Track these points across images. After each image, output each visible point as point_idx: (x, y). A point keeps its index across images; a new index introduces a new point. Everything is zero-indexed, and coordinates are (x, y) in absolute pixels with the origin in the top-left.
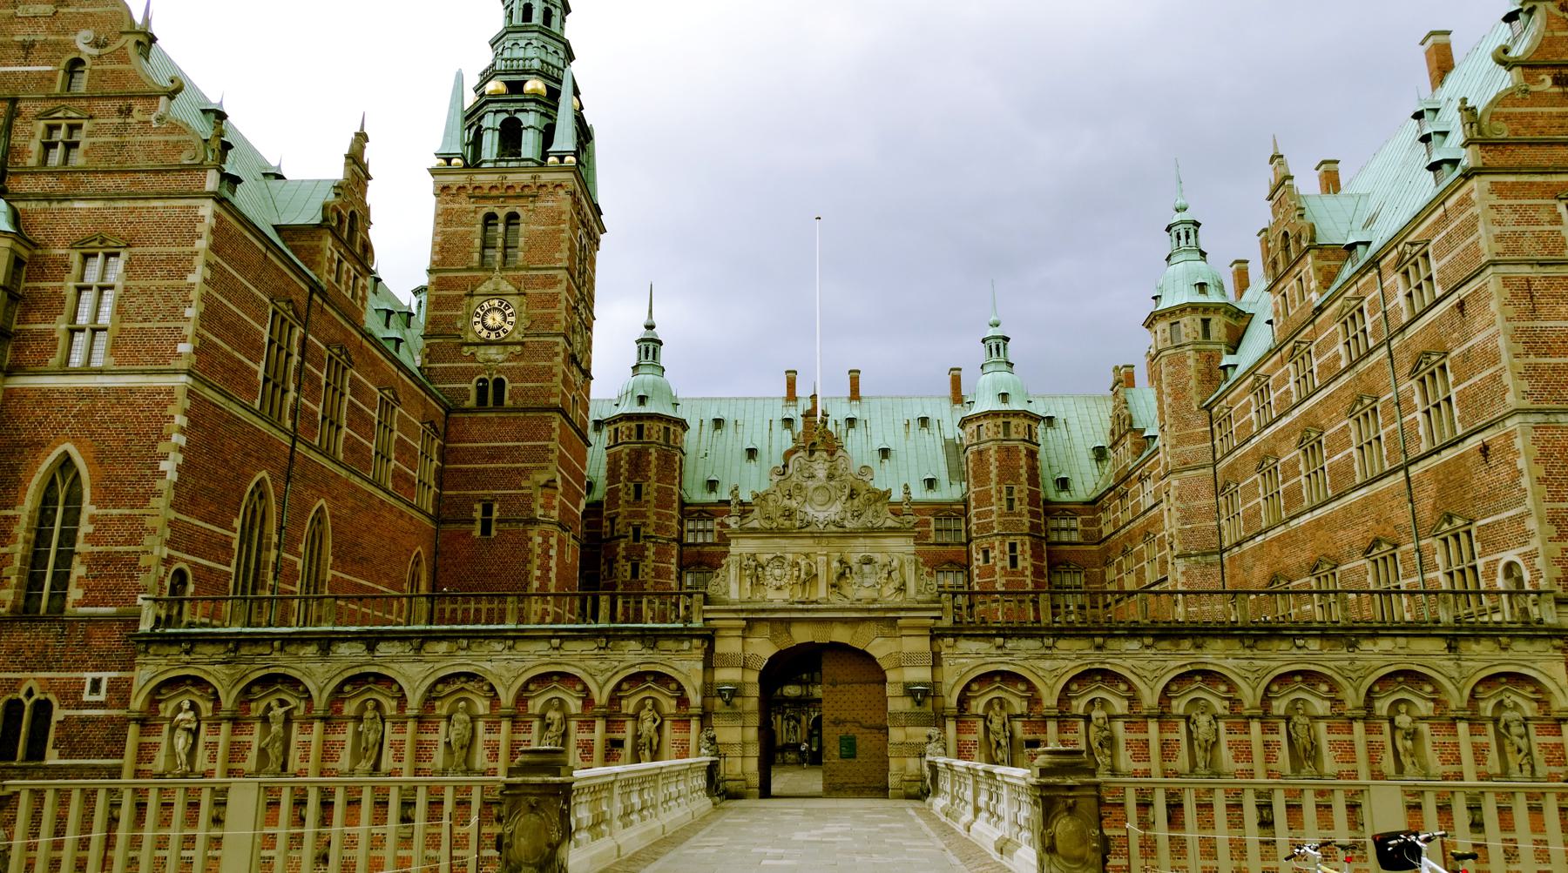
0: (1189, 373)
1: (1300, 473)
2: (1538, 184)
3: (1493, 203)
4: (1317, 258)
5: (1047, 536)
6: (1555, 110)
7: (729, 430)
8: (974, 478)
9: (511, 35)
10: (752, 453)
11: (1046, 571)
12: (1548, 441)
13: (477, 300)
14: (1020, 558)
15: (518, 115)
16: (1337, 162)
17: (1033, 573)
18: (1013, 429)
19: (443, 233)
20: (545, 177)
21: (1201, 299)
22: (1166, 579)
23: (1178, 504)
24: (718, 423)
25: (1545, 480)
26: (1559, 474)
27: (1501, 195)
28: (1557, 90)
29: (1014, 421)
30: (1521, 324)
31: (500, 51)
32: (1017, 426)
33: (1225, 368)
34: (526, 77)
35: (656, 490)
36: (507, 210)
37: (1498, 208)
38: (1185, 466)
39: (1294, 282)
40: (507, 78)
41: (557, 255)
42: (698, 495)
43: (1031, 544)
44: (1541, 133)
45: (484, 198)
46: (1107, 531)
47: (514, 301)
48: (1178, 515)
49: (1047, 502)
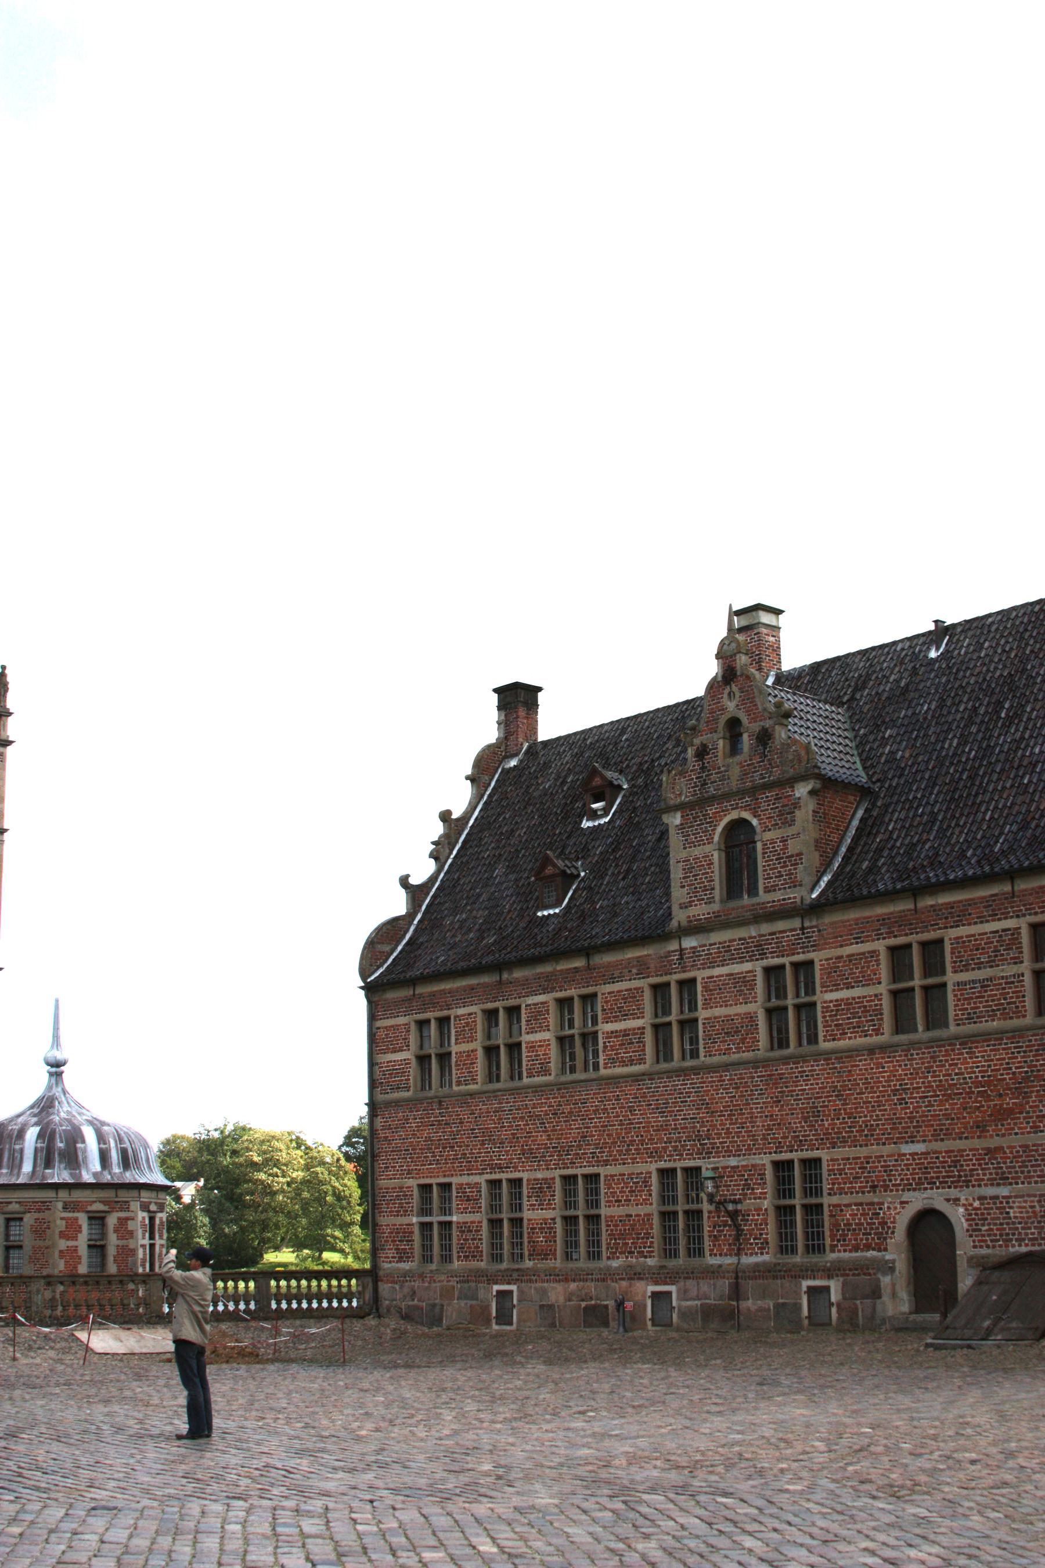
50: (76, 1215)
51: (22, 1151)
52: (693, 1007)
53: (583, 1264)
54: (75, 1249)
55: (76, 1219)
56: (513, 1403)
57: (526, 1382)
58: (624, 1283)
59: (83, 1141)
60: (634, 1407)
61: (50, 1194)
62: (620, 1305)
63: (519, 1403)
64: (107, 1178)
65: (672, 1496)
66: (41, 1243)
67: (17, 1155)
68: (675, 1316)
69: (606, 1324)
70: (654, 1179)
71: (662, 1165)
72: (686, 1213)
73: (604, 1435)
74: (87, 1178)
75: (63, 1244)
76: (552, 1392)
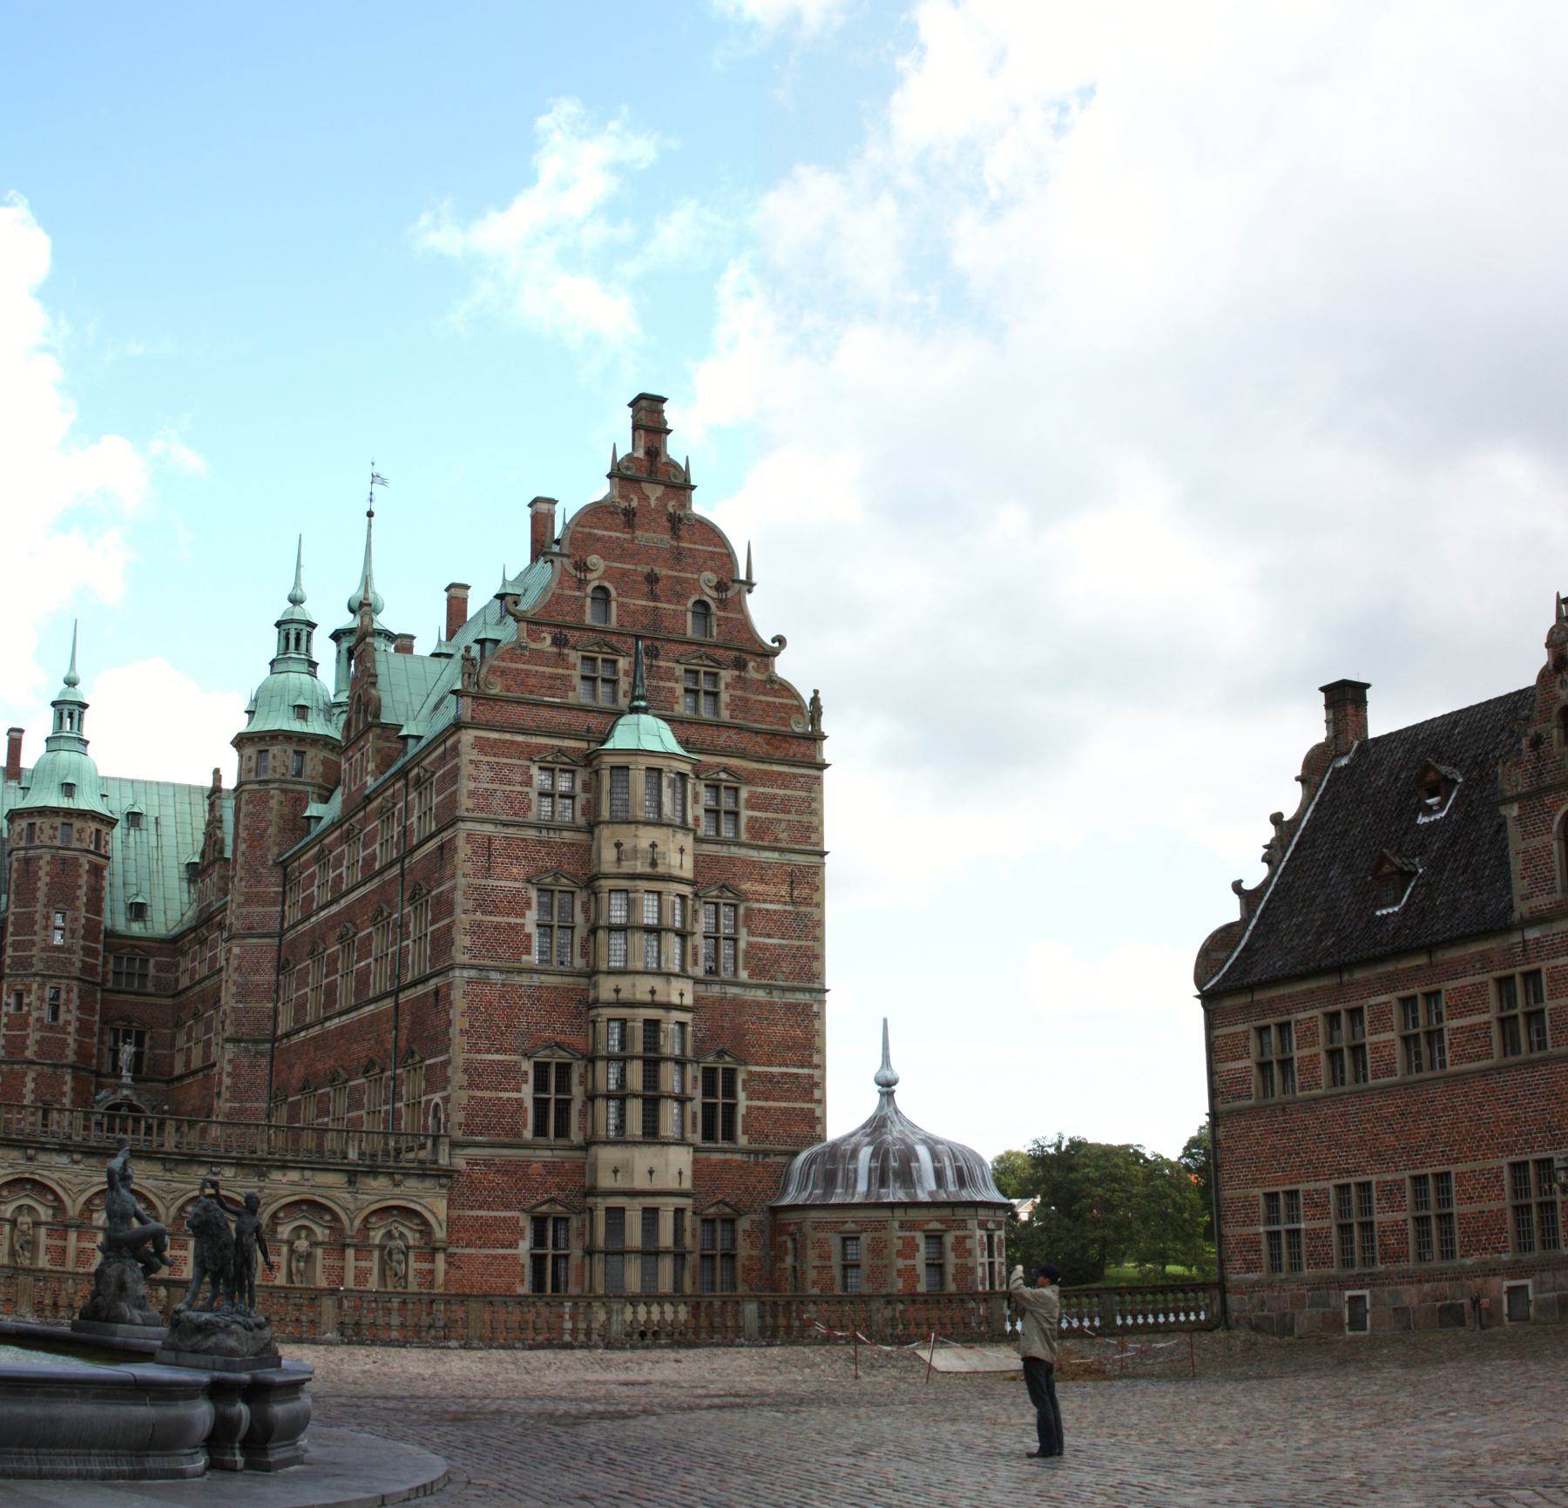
0: (269, 817)
1: (337, 972)
2: (518, 743)
3: (472, 758)
4: (379, 737)
5: (105, 980)
6: (548, 670)
8: (17, 893)
11: (96, 1029)
12: (477, 996)
14: (63, 1009)
16: (467, 587)
17: (78, 1031)
18: (76, 835)
21: (297, 726)
22: (214, 1065)
23: (235, 977)
25: (467, 1032)
26: (480, 1027)
27: (482, 750)
28: (555, 650)
29: (77, 824)
30: (477, 881)
32: (81, 831)
33: (309, 818)
37: (476, 763)
38: (250, 932)
39: (358, 755)
43: (80, 991)
44: (531, 692)
46: (185, 982)
48: (233, 989)
49: (111, 934)
50: (912, 1234)
51: (856, 1171)
52: (1538, 998)
53: (1436, 1263)
54: (913, 1268)
55: (913, 1238)
56: (1371, 1408)
57: (1383, 1387)
58: (1479, 1281)
59: (918, 1160)
60: (1495, 1404)
61: (886, 1213)
62: (1476, 1302)
63: (1378, 1408)
64: (943, 1196)
65: (1539, 1489)
66: (880, 1262)
67: (851, 1175)
68: (1532, 1310)
69: (1462, 1323)
70: (1506, 1174)
71: (1514, 1159)
72: (1540, 1205)
73: (1469, 1434)
74: (923, 1197)
75: (901, 1263)
76: (1411, 1395)
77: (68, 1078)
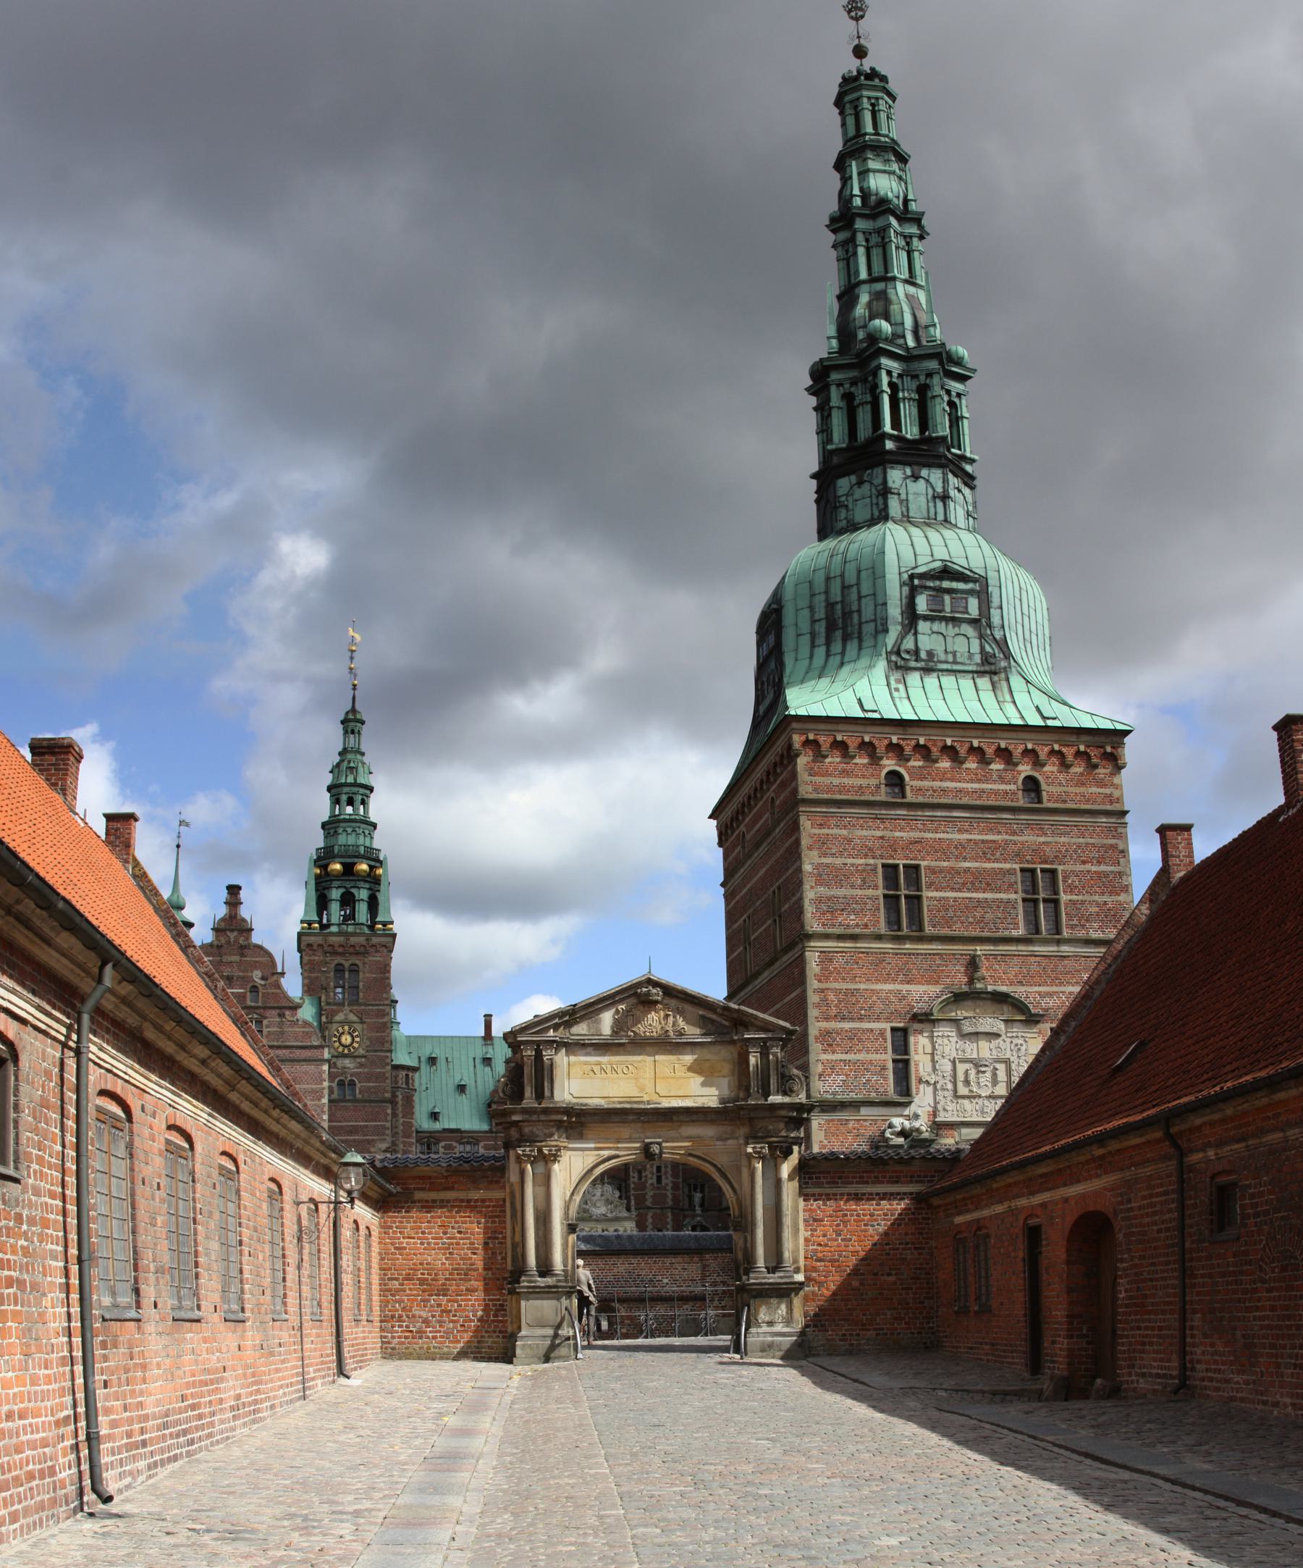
7: (441, 1063)
9: (342, 824)
10: (462, 1088)
13: (335, 1026)
15: (353, 890)
19: (309, 978)
20: (375, 940)
24: (432, 1061)
31: (332, 831)
34: (356, 860)
35: (403, 1125)
36: (350, 962)
40: (343, 860)
41: (384, 995)
42: (426, 1124)
45: (335, 953)
47: (359, 1027)
77: (669, 1214)
